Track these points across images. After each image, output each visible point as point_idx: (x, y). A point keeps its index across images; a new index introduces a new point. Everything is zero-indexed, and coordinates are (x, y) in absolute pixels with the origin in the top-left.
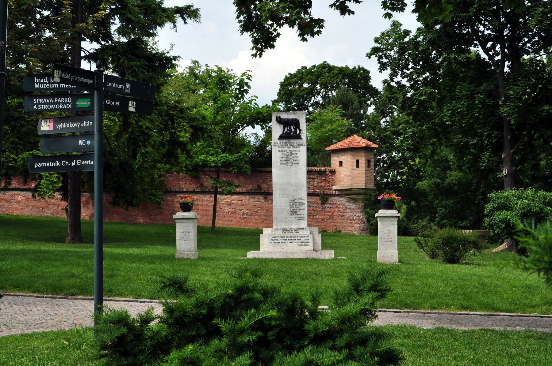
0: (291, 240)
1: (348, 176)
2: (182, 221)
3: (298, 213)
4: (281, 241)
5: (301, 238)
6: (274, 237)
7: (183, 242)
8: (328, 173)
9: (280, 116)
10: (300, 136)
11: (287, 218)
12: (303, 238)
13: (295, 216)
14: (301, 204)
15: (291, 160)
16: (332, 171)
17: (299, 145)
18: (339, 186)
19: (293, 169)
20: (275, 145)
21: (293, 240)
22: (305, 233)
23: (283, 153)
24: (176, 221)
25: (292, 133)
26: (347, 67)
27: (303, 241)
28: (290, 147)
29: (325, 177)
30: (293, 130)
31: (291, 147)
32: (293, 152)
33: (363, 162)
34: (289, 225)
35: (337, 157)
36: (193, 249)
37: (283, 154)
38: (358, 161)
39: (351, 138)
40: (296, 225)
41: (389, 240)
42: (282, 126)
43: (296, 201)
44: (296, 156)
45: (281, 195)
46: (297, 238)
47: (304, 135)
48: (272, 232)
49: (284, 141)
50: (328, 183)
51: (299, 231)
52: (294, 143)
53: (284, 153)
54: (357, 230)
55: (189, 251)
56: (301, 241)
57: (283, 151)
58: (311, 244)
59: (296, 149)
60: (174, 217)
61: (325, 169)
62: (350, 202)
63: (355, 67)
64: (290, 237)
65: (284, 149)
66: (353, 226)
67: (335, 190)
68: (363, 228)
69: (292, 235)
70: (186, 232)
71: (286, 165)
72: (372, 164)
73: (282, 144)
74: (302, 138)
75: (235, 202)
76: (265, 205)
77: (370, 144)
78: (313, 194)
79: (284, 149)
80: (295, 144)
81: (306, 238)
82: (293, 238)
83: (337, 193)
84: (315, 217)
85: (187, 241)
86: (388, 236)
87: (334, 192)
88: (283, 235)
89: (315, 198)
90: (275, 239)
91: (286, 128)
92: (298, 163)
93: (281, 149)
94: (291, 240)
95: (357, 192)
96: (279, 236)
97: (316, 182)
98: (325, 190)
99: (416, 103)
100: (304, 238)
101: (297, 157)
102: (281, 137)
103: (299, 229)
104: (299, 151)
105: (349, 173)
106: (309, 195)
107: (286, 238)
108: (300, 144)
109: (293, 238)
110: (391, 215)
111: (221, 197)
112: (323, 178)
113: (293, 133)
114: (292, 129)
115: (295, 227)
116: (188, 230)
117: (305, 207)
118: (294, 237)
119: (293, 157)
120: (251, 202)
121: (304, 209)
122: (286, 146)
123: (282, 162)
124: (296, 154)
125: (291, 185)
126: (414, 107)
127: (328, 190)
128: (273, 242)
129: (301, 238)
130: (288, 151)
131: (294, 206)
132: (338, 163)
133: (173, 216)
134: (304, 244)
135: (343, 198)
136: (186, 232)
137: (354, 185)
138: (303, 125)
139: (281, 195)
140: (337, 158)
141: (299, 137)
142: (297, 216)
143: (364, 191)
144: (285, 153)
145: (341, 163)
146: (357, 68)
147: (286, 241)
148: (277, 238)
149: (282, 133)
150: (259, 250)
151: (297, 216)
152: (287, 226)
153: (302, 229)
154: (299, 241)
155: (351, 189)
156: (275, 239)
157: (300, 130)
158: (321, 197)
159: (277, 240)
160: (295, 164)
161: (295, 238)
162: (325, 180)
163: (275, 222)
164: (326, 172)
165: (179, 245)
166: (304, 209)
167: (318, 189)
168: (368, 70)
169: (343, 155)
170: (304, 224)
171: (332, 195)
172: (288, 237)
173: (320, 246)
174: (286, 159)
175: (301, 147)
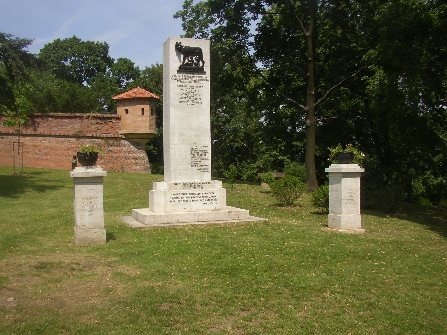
1: (134, 122)
3: (201, 164)
4: (183, 199)
6: (175, 194)
7: (87, 213)
9: (180, 43)
12: (209, 195)
15: (192, 98)
20: (173, 79)
21: (198, 197)
23: (182, 88)
25: (194, 65)
27: (209, 198)
30: (195, 61)
32: (195, 89)
38: (143, 110)
39: (135, 90)
40: (198, 179)
43: (198, 149)
44: (199, 93)
46: (201, 195)
51: (203, 185)
55: (96, 226)
56: (206, 198)
57: (182, 86)
59: (199, 85)
65: (184, 84)
67: (121, 134)
73: (181, 77)
74: (205, 72)
75: (27, 143)
76: (56, 146)
79: (184, 84)
80: (197, 80)
81: (212, 195)
82: (197, 195)
83: (123, 137)
84: (103, 157)
87: (120, 136)
88: (185, 191)
90: (175, 196)
92: (201, 103)
93: (180, 84)
95: (142, 136)
100: (210, 195)
102: (181, 70)
104: (202, 87)
107: (188, 196)
108: (203, 79)
109: (197, 195)
111: (13, 139)
113: (196, 64)
114: (194, 59)
115: (198, 181)
117: (209, 156)
118: (198, 194)
120: (43, 143)
121: (207, 159)
122: (187, 81)
123: (182, 100)
128: (172, 200)
132: (124, 112)
134: (210, 202)
136: (91, 198)
141: (201, 71)
142: (199, 168)
144: (185, 88)
145: (127, 111)
148: (177, 196)
151: (199, 168)
154: (204, 199)
156: (175, 196)
157: (203, 62)
160: (197, 103)
161: (199, 195)
163: (174, 175)
166: (207, 159)
170: (208, 176)
174: (186, 96)
175: (203, 82)
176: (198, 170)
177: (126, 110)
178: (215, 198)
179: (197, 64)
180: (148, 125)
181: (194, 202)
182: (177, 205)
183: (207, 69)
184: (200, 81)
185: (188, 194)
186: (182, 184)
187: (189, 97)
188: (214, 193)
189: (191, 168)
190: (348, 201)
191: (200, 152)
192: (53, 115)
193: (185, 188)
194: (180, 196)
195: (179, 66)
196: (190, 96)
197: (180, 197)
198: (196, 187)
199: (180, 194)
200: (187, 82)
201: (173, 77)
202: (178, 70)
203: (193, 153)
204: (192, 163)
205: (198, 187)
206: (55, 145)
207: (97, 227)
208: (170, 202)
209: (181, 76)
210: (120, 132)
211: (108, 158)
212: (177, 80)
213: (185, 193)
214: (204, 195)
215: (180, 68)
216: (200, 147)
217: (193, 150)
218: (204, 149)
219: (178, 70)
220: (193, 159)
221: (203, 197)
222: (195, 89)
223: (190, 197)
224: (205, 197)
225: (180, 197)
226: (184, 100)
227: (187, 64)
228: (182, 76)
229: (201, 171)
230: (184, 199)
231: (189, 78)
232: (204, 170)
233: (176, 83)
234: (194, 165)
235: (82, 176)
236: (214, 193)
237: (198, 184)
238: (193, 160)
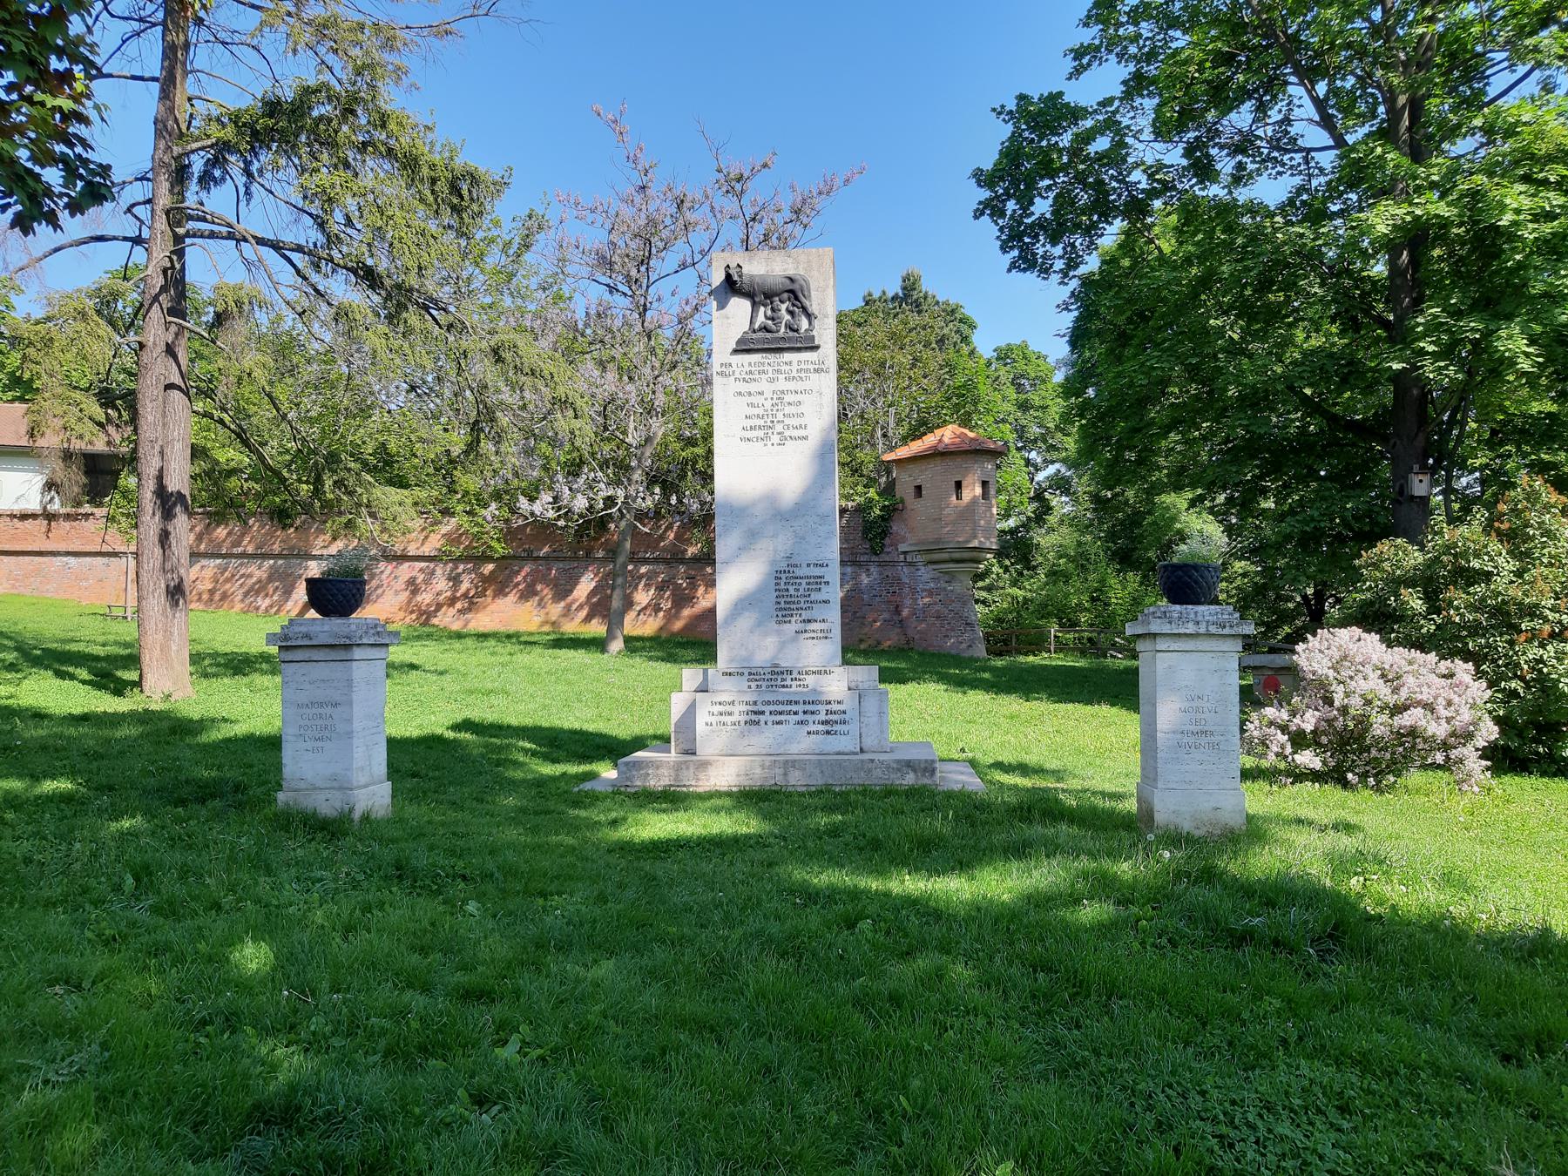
0: (781, 713)
17: (807, 371)
21: (789, 713)
27: (823, 717)
32: (788, 398)
37: (751, 405)
41: (1203, 740)
43: (799, 572)
59: (799, 386)
71: (761, 444)
79: (753, 387)
80: (795, 371)
82: (789, 708)
100: (829, 707)
108: (811, 367)
109: (789, 708)
114: (783, 312)
118: (790, 702)
119: (789, 416)
130: (768, 394)
131: (792, 592)
136: (321, 705)
147: (762, 718)
149: (746, 327)
156: (721, 708)
161: (794, 708)
172: (768, 703)
174: (762, 422)
175: (814, 376)
178: (843, 716)
183: (826, 333)
184: (803, 375)
191: (804, 582)
193: (753, 685)
197: (737, 713)
200: (764, 381)
204: (780, 614)
209: (746, 365)
214: (807, 707)
216: (804, 565)
217: (783, 576)
218: (817, 572)
221: (805, 712)
222: (788, 398)
223: (767, 713)
224: (813, 713)
228: (750, 364)
231: (770, 369)
238: (783, 605)
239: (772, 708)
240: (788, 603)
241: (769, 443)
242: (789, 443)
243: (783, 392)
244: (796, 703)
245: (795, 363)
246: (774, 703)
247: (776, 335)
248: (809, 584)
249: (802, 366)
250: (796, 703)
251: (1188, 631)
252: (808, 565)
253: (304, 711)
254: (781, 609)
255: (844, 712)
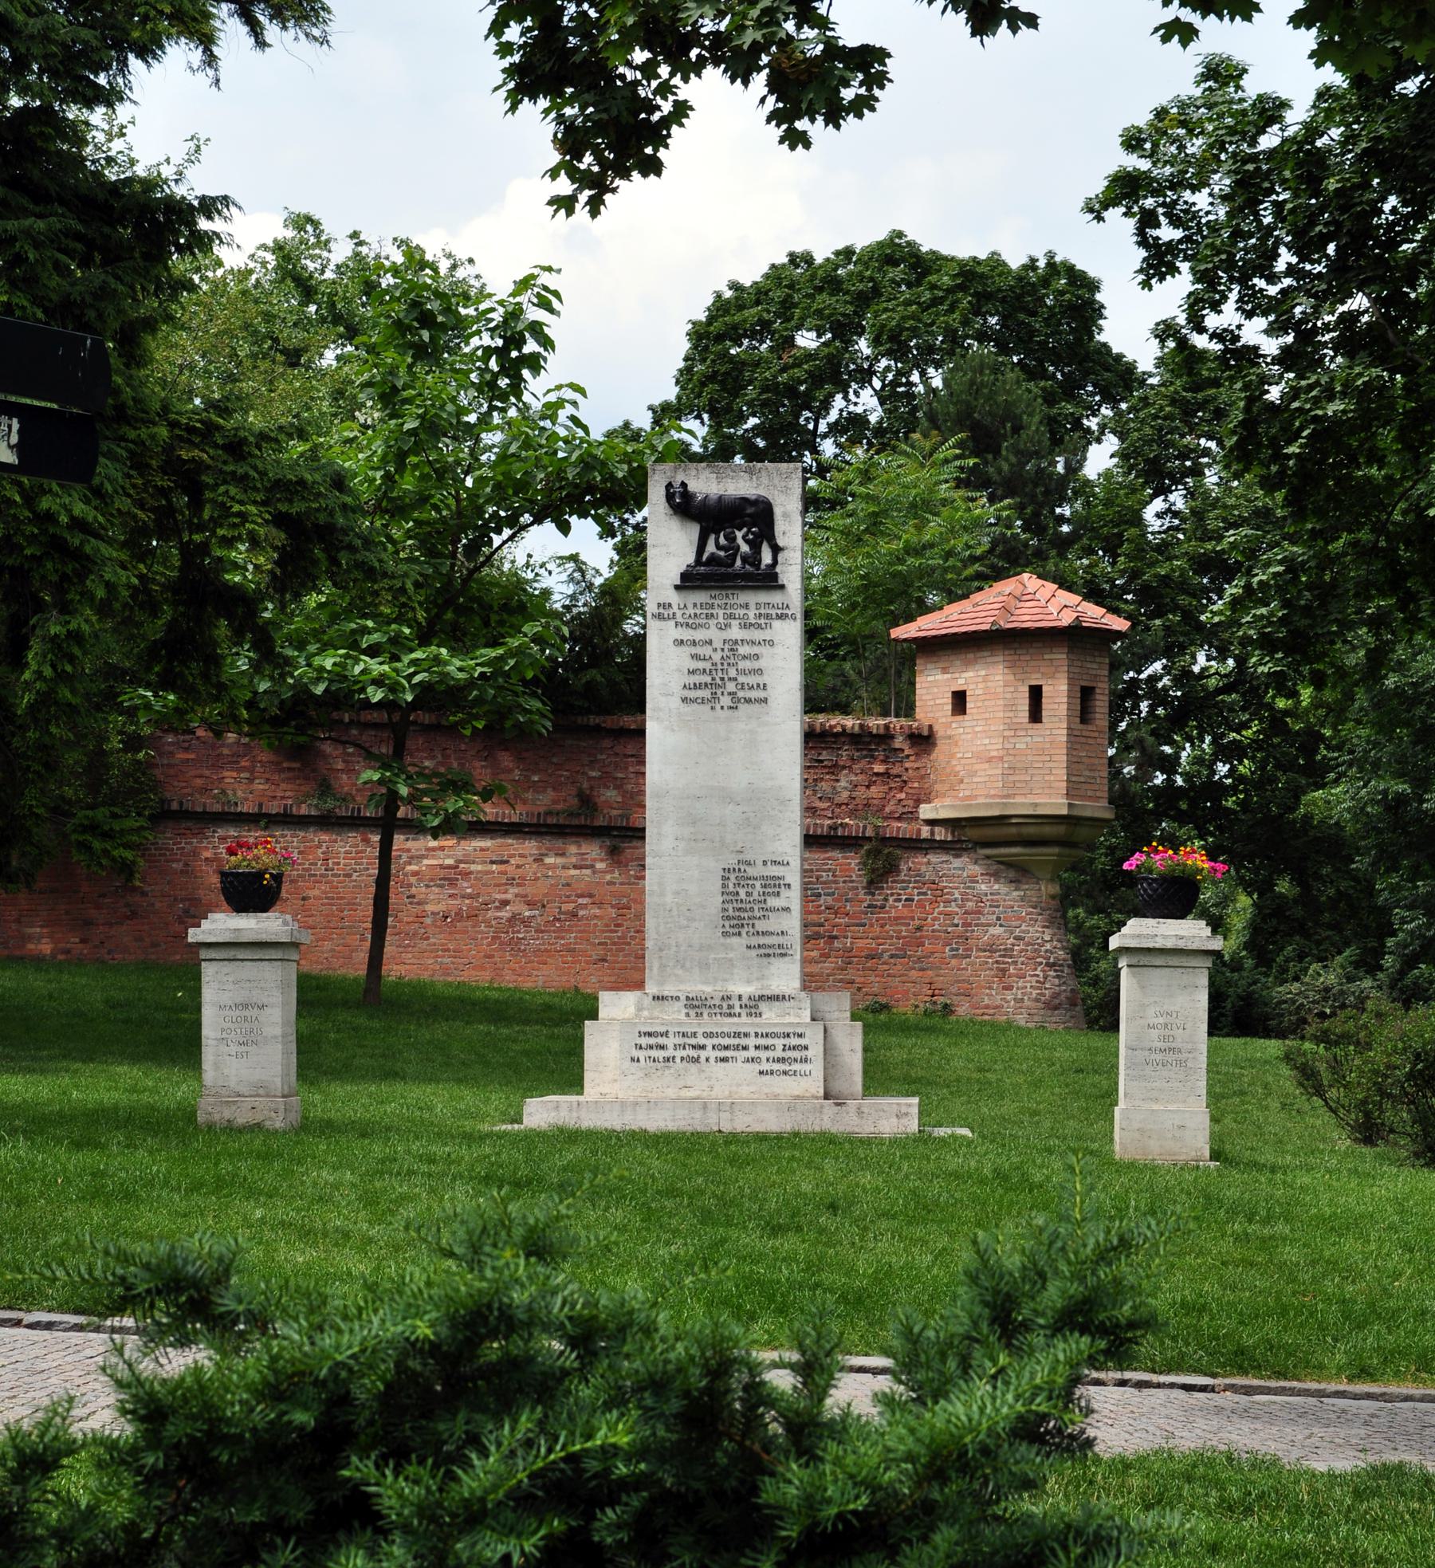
0: (726, 1048)
1: (990, 760)
2: (231, 953)
3: (761, 926)
5: (769, 1042)
6: (650, 1034)
8: (899, 742)
9: (684, 485)
10: (775, 576)
11: (710, 948)
12: (779, 1043)
13: (743, 941)
14: (774, 885)
16: (920, 736)
17: (768, 616)
18: (948, 801)
19: (742, 726)
20: (660, 617)
21: (737, 1048)
22: (787, 1020)
23: (694, 650)
24: (204, 954)
25: (738, 563)
26: (995, 262)
27: (779, 1053)
28: (728, 626)
29: (884, 761)
30: (745, 548)
31: (735, 623)
32: (743, 650)
33: (1058, 694)
34: (716, 980)
35: (945, 671)
36: (278, 1081)
37: (695, 657)
38: (1036, 693)
39: (1007, 586)
40: (749, 982)
41: (1170, 1057)
42: (694, 530)
43: (751, 871)
44: (756, 665)
45: (682, 845)
46: (751, 1042)
47: (791, 574)
48: (639, 1009)
49: (701, 597)
50: (901, 790)
51: (763, 1007)
52: (747, 606)
53: (699, 650)
54: (1027, 1003)
55: (261, 1089)
56: (770, 1054)
57: (694, 643)
58: (816, 1068)
59: (758, 635)
60: (194, 935)
61: (887, 727)
62: (996, 876)
63: (1033, 260)
64: (723, 1035)
65: (699, 635)
66: (1009, 988)
67: (932, 823)
68: (1055, 995)
69: (728, 1024)
70: (245, 1006)
71: (707, 707)
72: (1101, 704)
74: (782, 587)
75: (473, 867)
76: (610, 883)
77: (1094, 614)
78: (828, 837)
79: (699, 635)
80: (751, 614)
81: (795, 1041)
82: (736, 1041)
83: (941, 834)
85: (251, 1049)
86: (1165, 1038)
87: (925, 831)
88: (692, 1025)
89: (837, 854)
90: (652, 1041)
91: (712, 538)
92: (765, 701)
93: (686, 634)
94: (726, 1048)
96: (672, 1030)
97: (843, 784)
98: (886, 818)
99: (1302, 428)
100: (786, 1041)
101: (759, 672)
102: (689, 581)
103: (761, 997)
104: (771, 643)
105: (995, 747)
106: (811, 841)
107: (701, 1041)
108: (773, 612)
109: (736, 1041)
110: (1181, 944)
111: (410, 844)
112: (879, 768)
113: (744, 560)
114: (740, 541)
115: (748, 990)
116: (258, 997)
117: (793, 898)
118: (737, 1035)
119: (743, 672)
121: (787, 909)
122: (712, 622)
123: (693, 694)
124: (757, 657)
125: (728, 797)
126: (1293, 449)
127: (899, 819)
128: (641, 1054)
129: (769, 1042)
130: (718, 644)
133: (191, 931)
135: (965, 859)
136: (245, 1006)
137: (1019, 800)
138: (789, 527)
139: (682, 845)
140: (940, 677)
141: (769, 580)
142: (755, 941)
143: (1060, 830)
144: (706, 651)
145: (959, 700)
146: (1042, 263)
147: (703, 1054)
148: (661, 1041)
149: (691, 559)
150: (581, 1093)
151: (755, 941)
152: (706, 983)
153: (776, 998)
154: (763, 1055)
155: (1001, 820)
156: (652, 1041)
157: (776, 550)
158: (869, 853)
159: (662, 1047)
160: (748, 701)
161: (743, 1041)
162: (887, 774)
163: (656, 965)
164: (892, 737)
165: (216, 1066)
166: (787, 909)
167: (852, 814)
168: (1092, 273)
169: (968, 664)
170: (786, 976)
171: (916, 845)
172: (711, 1035)
173: (858, 1079)
174: (708, 679)
175: (777, 624)
176: (749, 947)
177: (1031, 687)
178: (804, 1053)
179: (754, 559)
180: (1059, 774)
181: (723, 1065)
182: (659, 1073)
184: (762, 621)
185: (699, 1035)
186: (683, 998)
187: (718, 681)
188: (800, 1036)
189: (722, 940)
190: (1153, 1056)
191: (758, 884)
192: (598, 725)
193: (692, 1013)
194: (670, 1042)
195: (683, 568)
196: (722, 679)
197: (671, 1046)
198: (737, 1010)
199: (671, 1035)
200: (713, 627)
201: (661, 610)
202: (678, 582)
203: (731, 885)
204: (727, 924)
205: (744, 1012)
206: (608, 877)
207: (261, 1091)
208: (633, 1059)
209: (690, 606)
210: (926, 811)
211: (860, 943)
212: (672, 623)
213: (690, 1030)
215: (685, 576)
216: (759, 863)
217: (732, 877)
219: (678, 582)
220: (730, 907)
221: (757, 1047)
223: (709, 1048)
224: (766, 1048)
225: (671, 1046)
226: (699, 693)
227: (713, 559)
228: (695, 605)
229: (762, 951)
230: (684, 1053)
231: (721, 612)
232: (771, 951)
233: (672, 632)
234: (736, 930)
235: (221, 940)
236: (800, 1036)
237: (745, 1001)
238: (731, 912)
239: (715, 1041)
240: (739, 909)
241: (718, 707)
242: (742, 707)
243: (736, 642)
244: (746, 1035)
245: (752, 606)
246: (718, 1035)
247: (730, 570)
248: (765, 886)
249: (763, 611)
250: (746, 1035)
251: (1157, 946)
252: (765, 863)
253: (227, 1013)
254: (728, 918)
255: (806, 1048)
